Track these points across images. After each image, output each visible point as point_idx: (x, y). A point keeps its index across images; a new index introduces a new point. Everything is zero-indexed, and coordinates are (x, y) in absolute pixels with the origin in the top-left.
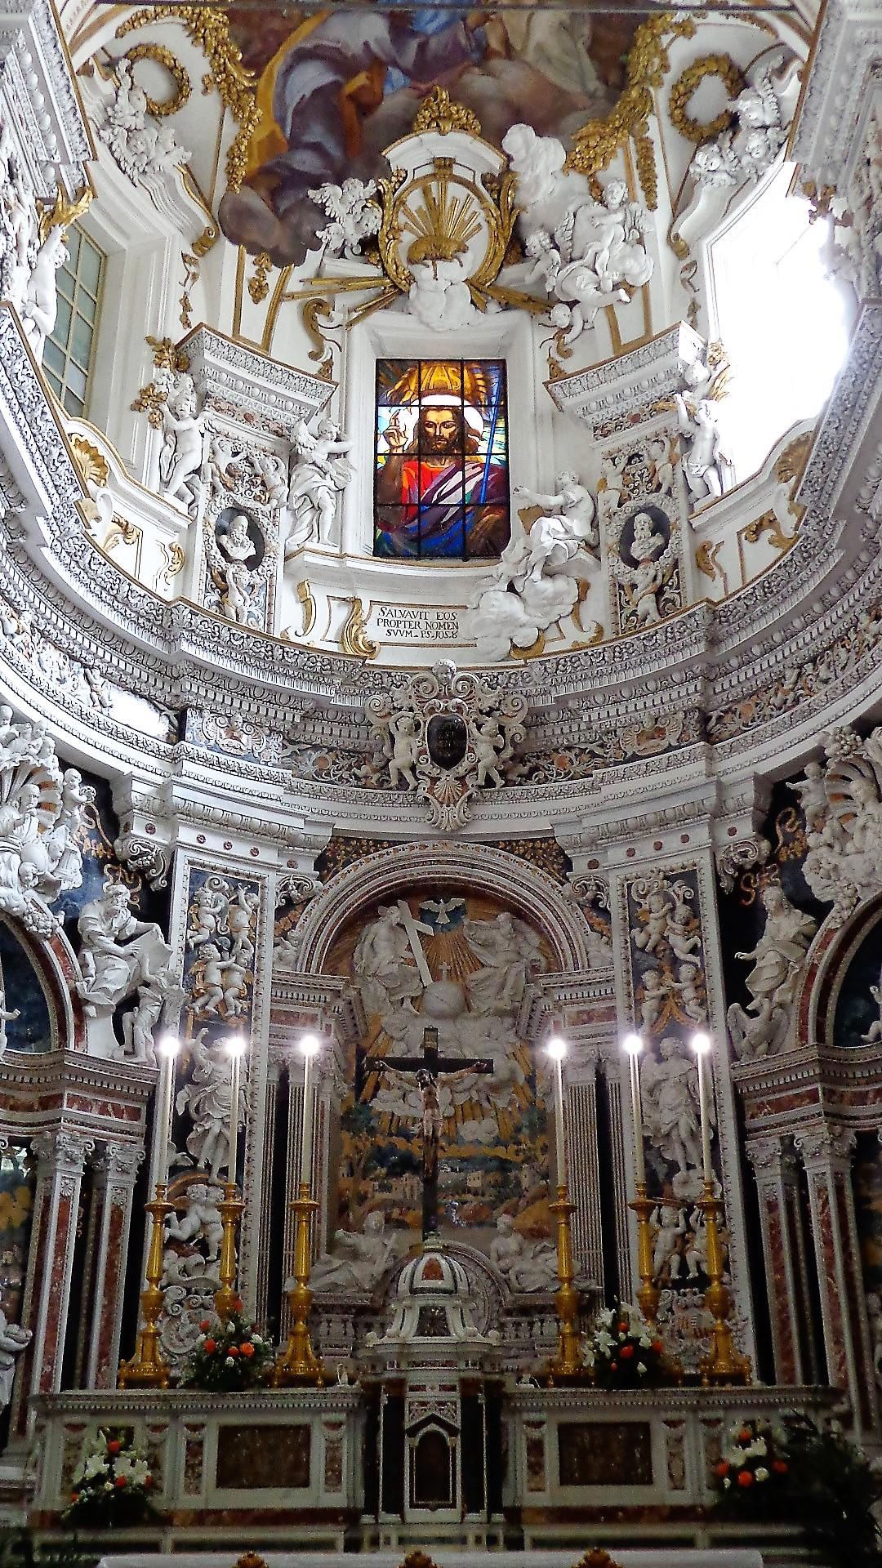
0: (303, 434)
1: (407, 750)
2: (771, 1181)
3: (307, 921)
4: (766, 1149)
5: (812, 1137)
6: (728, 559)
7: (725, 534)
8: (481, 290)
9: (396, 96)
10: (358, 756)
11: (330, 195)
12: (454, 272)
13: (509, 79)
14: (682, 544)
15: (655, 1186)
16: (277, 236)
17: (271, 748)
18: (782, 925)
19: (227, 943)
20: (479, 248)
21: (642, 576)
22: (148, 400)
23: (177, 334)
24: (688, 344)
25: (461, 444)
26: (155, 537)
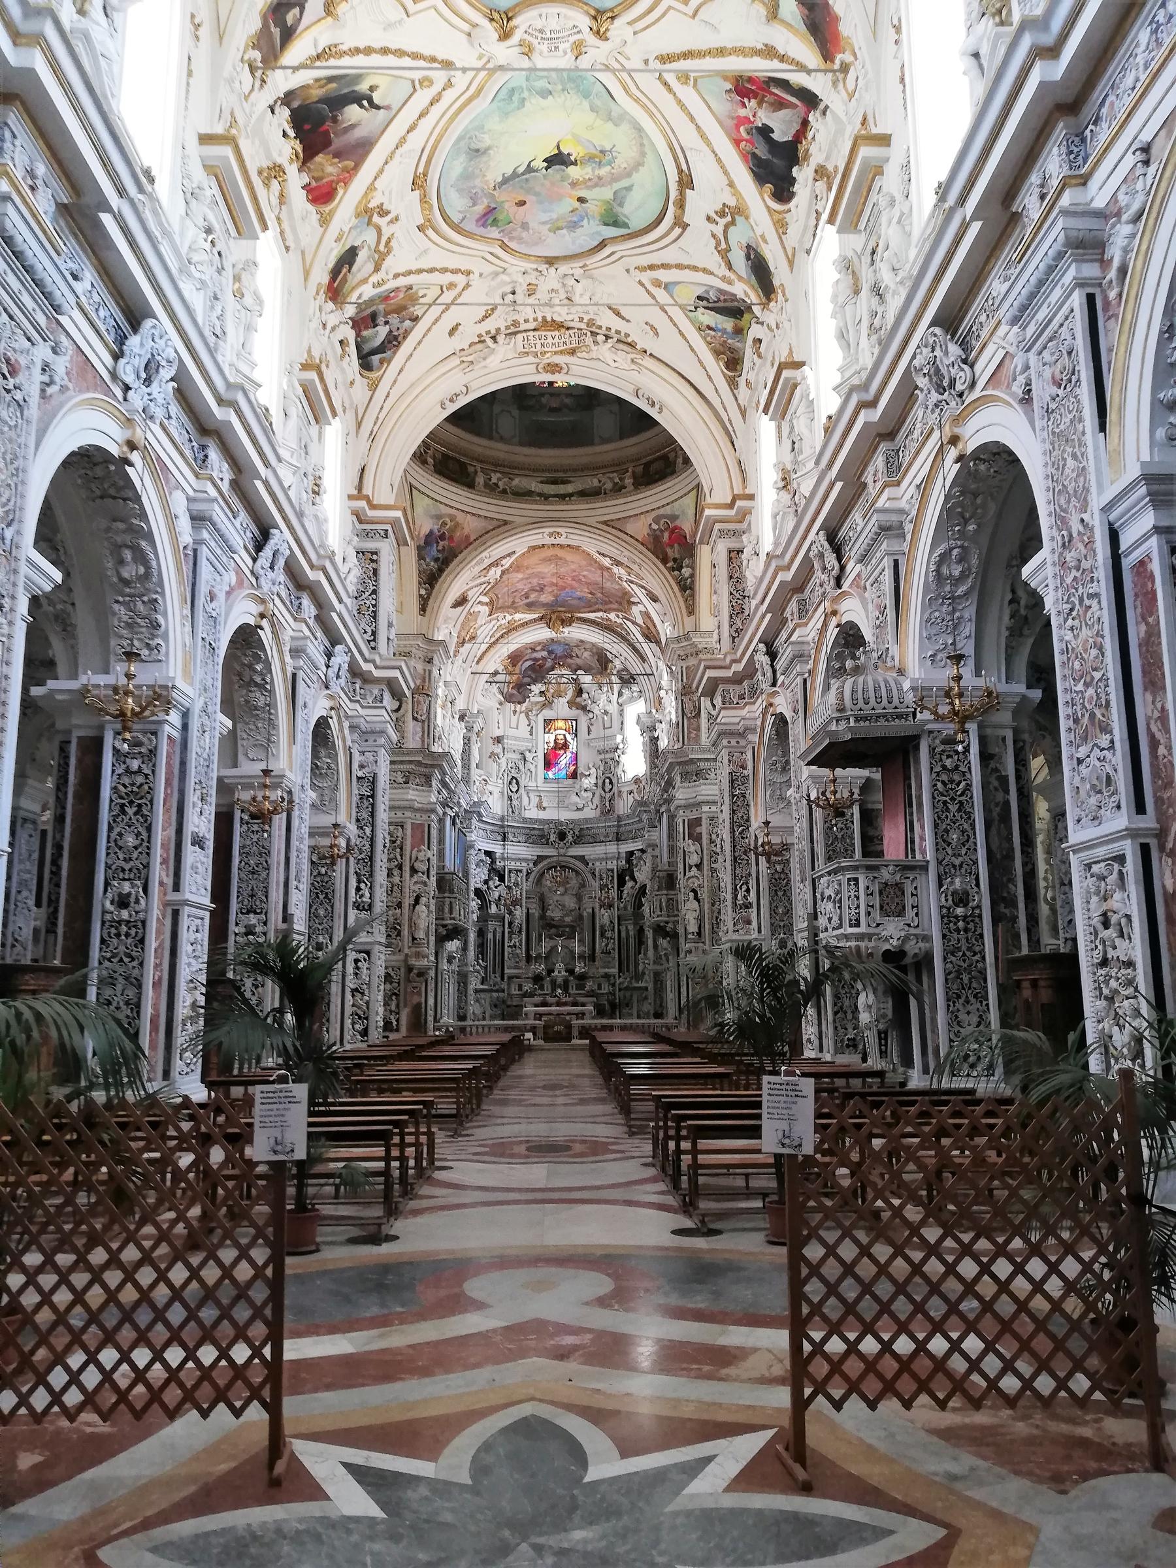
0: (527, 754)
1: (553, 838)
2: (623, 934)
3: (532, 876)
4: (623, 929)
5: (631, 927)
6: (625, 795)
7: (625, 790)
8: (571, 704)
9: (549, 663)
10: (542, 837)
11: (533, 687)
12: (563, 701)
13: (578, 661)
14: (615, 789)
15: (602, 935)
16: (520, 698)
17: (522, 838)
18: (630, 884)
19: (516, 884)
20: (570, 693)
21: (608, 796)
22: (493, 755)
23: (498, 733)
24: (619, 738)
25: (565, 746)
26: (496, 791)
